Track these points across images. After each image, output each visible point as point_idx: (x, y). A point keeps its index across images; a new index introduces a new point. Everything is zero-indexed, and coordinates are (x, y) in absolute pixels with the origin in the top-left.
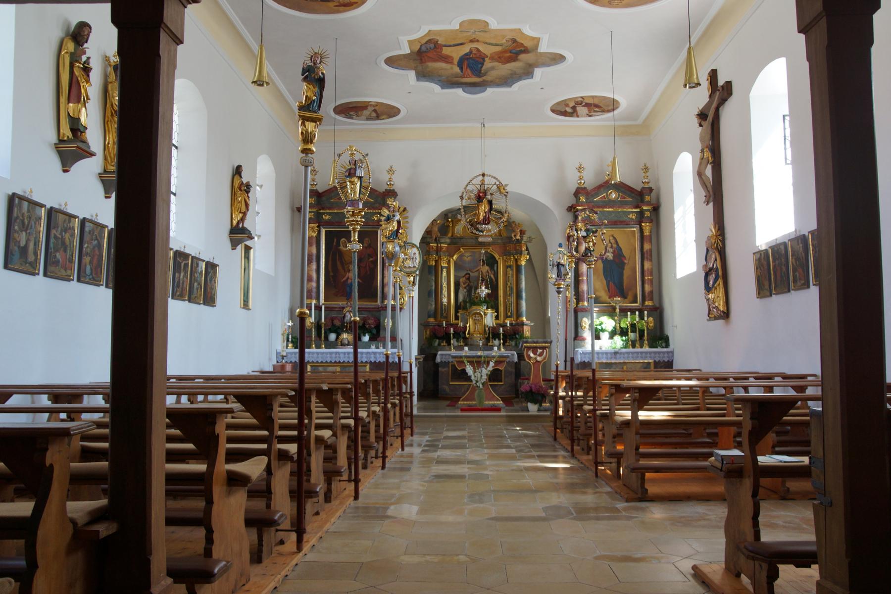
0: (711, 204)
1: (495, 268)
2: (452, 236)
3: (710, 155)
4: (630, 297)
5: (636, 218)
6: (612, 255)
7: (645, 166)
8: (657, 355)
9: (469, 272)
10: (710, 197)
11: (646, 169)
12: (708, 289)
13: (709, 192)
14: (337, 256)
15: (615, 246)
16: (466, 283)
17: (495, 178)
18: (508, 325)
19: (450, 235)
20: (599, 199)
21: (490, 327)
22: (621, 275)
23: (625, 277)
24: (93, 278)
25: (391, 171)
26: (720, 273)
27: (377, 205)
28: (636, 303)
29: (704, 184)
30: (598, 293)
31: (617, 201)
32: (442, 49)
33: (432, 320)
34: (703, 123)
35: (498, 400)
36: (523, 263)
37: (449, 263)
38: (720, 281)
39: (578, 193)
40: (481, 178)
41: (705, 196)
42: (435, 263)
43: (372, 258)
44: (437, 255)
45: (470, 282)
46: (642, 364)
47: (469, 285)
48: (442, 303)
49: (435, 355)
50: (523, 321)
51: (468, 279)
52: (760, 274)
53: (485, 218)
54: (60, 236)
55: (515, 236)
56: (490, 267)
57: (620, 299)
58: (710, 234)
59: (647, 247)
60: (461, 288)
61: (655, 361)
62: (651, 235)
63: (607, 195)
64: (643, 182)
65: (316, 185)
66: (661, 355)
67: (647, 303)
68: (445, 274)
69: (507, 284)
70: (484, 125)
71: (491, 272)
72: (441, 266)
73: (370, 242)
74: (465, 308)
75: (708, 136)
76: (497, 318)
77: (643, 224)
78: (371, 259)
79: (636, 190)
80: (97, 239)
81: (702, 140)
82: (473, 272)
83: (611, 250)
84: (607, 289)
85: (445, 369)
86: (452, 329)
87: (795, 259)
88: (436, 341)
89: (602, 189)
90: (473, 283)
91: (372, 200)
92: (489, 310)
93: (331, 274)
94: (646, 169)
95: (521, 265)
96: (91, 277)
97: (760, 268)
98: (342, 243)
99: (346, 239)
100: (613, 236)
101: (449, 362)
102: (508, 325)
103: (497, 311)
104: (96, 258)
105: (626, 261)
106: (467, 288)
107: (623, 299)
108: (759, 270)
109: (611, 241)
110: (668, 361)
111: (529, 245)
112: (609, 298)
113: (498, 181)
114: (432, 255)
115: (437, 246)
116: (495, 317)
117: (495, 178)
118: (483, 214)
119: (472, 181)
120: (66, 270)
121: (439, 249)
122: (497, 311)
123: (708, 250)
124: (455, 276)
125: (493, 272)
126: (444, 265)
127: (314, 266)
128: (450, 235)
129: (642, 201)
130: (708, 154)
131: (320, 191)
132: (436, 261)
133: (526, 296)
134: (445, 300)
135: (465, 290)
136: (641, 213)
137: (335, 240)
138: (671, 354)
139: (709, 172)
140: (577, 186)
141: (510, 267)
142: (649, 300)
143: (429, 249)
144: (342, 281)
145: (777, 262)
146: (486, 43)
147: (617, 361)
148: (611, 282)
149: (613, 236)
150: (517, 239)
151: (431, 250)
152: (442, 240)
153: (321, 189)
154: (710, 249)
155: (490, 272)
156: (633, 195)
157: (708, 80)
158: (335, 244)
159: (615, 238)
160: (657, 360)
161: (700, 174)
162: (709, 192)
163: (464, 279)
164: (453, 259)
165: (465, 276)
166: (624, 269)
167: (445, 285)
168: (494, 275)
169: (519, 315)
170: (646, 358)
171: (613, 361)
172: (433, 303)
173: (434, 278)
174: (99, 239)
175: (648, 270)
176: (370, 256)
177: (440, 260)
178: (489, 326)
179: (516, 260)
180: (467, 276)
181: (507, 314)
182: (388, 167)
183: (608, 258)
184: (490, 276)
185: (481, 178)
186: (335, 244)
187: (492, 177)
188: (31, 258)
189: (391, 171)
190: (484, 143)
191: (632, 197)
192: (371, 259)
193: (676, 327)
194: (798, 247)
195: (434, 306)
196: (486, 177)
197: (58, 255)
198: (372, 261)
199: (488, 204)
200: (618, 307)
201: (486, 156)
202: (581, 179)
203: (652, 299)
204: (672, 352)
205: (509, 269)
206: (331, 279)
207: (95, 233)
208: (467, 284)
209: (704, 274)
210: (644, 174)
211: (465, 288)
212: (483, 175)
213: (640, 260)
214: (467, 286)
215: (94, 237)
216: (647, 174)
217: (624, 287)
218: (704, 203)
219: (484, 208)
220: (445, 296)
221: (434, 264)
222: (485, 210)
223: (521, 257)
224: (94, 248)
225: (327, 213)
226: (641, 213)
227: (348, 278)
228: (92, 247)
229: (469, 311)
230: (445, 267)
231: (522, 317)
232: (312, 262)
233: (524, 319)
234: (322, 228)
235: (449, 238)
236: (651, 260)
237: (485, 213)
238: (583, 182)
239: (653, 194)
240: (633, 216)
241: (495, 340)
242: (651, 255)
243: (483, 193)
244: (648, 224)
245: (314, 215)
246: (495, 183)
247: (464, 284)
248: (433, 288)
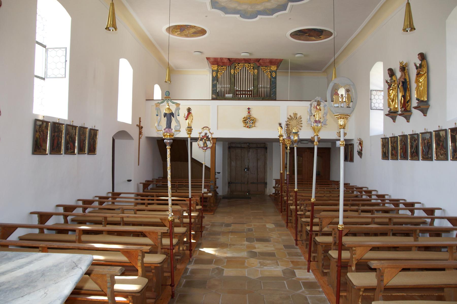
24: (404, 157)
52: (38, 137)
54: (393, 145)
80: (404, 142)
87: (69, 137)
96: (403, 157)
97: (39, 132)
104: (404, 149)
108: (38, 133)
120: (396, 157)
145: (56, 134)
174: (404, 141)
188: (387, 155)
194: (72, 131)
197: (393, 152)
207: (403, 140)
215: (403, 141)
224: (403, 145)
228: (402, 145)
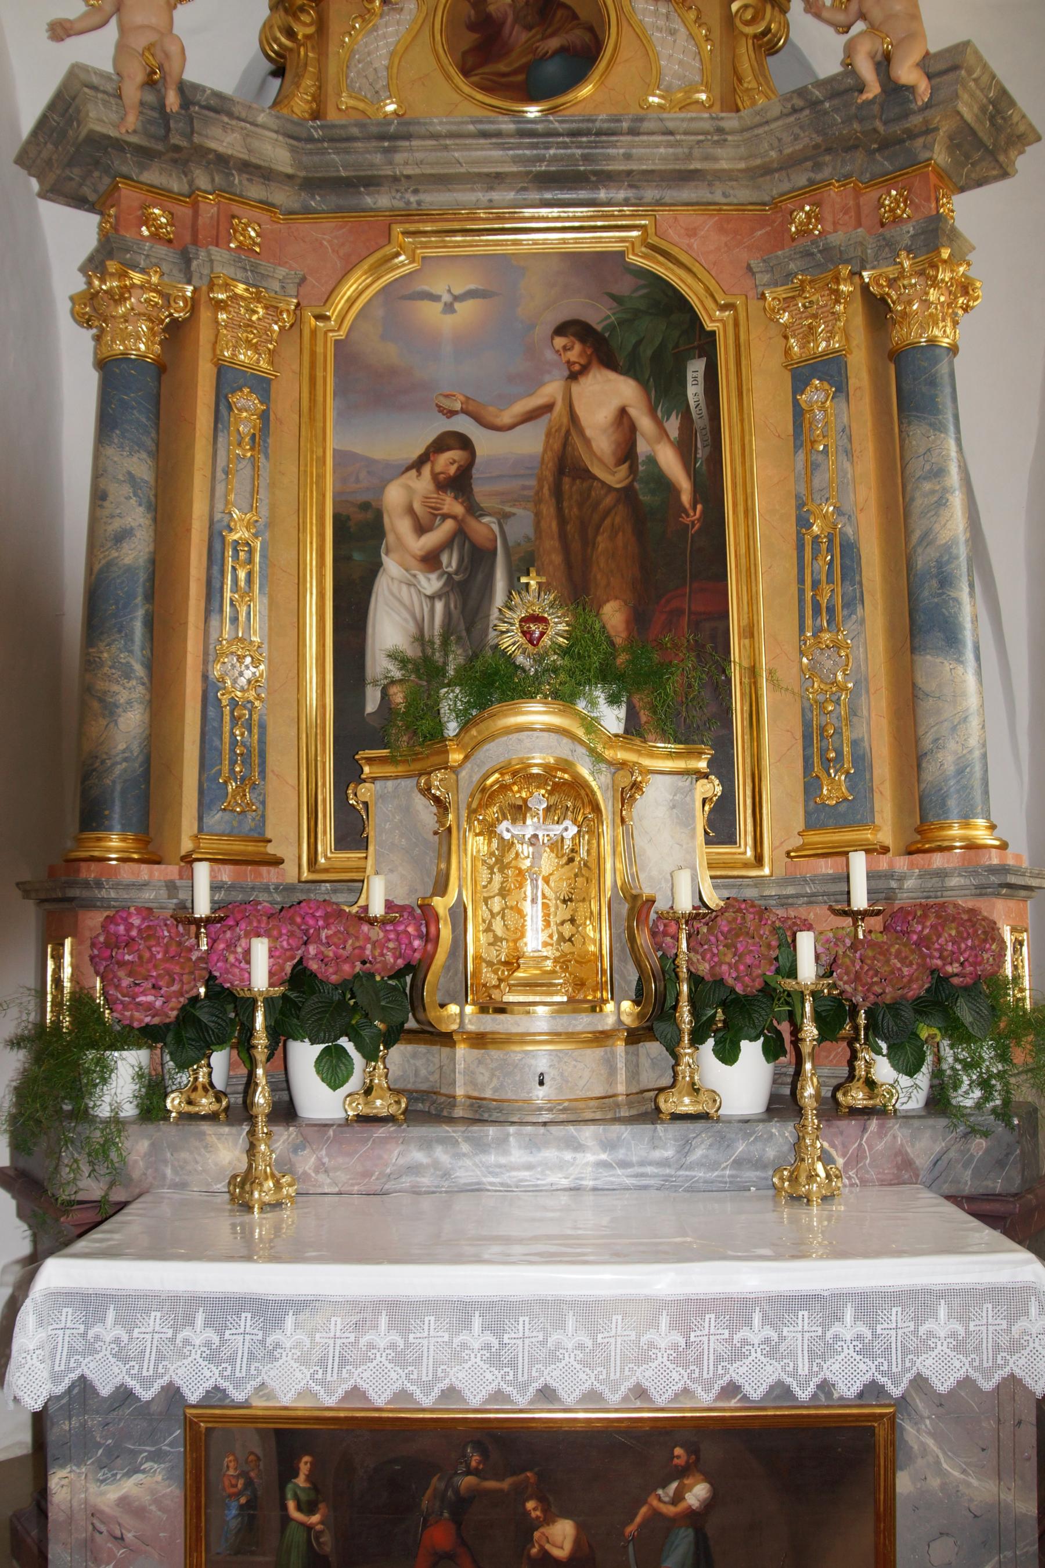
1: (694, 391)
9: (463, 425)
16: (437, 515)
18: (860, 901)
21: (672, 918)
45: (474, 509)
47: (460, 534)
48: (210, 689)
56: (643, 383)
60: (391, 566)
69: (803, 523)
71: (659, 424)
82: (511, 427)
85: (129, 1486)
86: (260, 949)
88: (105, 1071)
90: (503, 517)
102: (860, 901)
106: (450, 561)
116: (711, 822)
125: (673, 426)
126: (245, 356)
135: (431, 583)
155: (645, 423)
163: (422, 484)
165: (418, 464)
168: (685, 448)
177: (205, 314)
178: (661, 905)
180: (448, 461)
184: (652, 461)
205: (816, 394)
208: (449, 525)
211: (430, 560)
214: (447, 545)
230: (262, 386)
241: (728, 1054)
247: (421, 529)
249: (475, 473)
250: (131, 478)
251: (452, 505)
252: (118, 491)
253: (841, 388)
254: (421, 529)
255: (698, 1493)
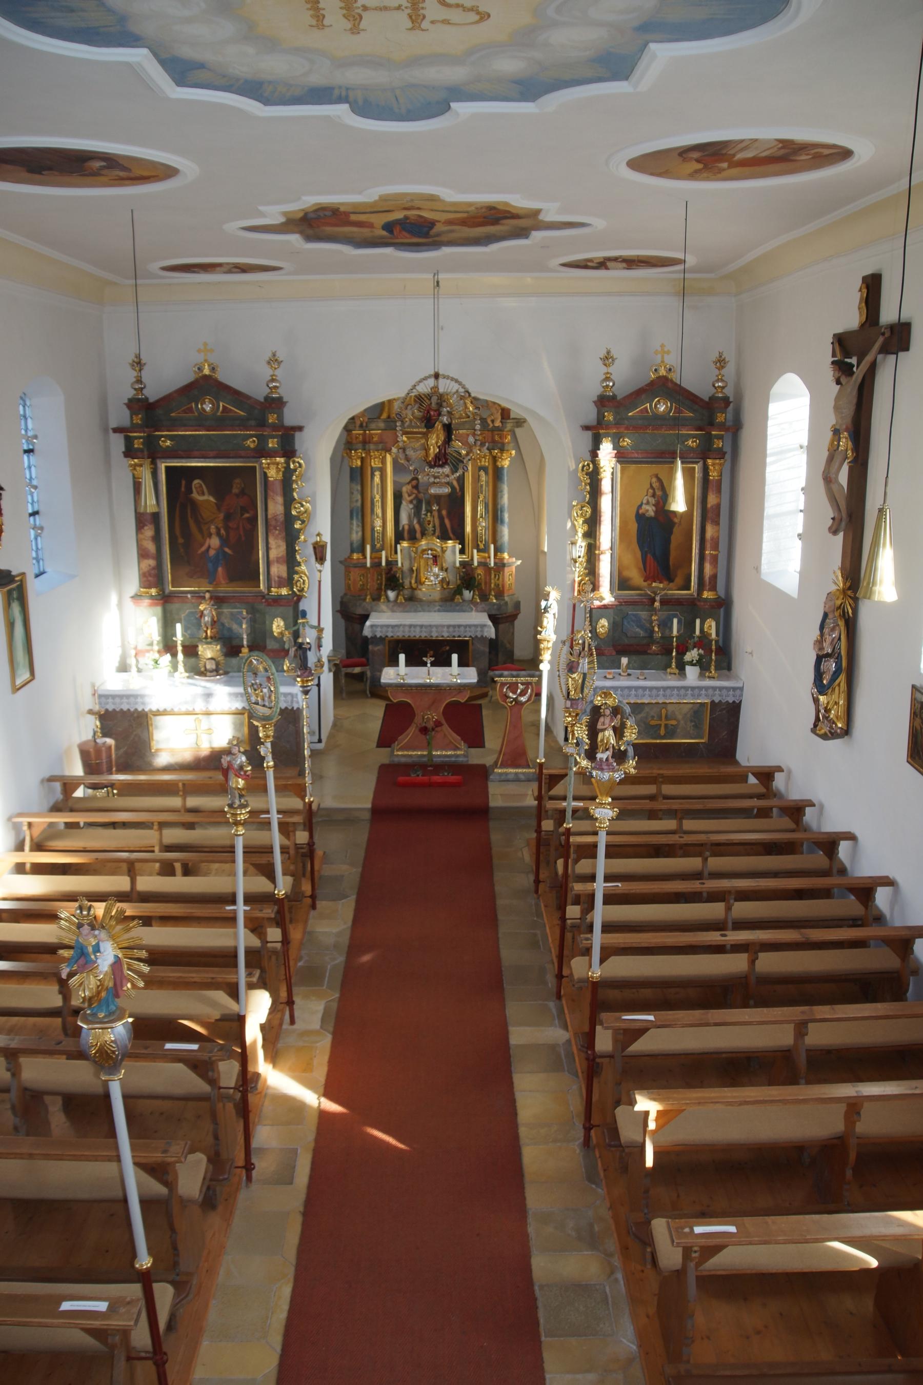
0: (841, 534)
2: (389, 417)
3: (850, 444)
4: (679, 580)
5: (698, 446)
6: (654, 508)
7: (721, 357)
8: (717, 692)
10: (841, 520)
11: (721, 362)
12: (820, 686)
13: (840, 510)
14: (189, 511)
15: (659, 493)
17: (457, 381)
19: (384, 416)
20: (638, 412)
22: (667, 542)
23: (673, 545)
25: (274, 361)
26: (844, 664)
27: (253, 423)
28: (689, 589)
29: (833, 499)
30: (626, 573)
31: (668, 417)
32: (349, 216)
33: (355, 556)
34: (843, 380)
35: (456, 748)
36: (506, 463)
37: (383, 461)
38: (842, 678)
39: (603, 401)
40: (431, 382)
41: (833, 519)
42: (362, 462)
43: (248, 513)
44: (364, 449)
45: (419, 492)
46: (691, 705)
47: (416, 498)
48: (373, 529)
49: (366, 617)
50: (504, 558)
51: (416, 487)
52: (919, 728)
53: (437, 457)
55: (493, 421)
57: (661, 586)
58: (834, 588)
59: (712, 500)
60: (404, 503)
61: (713, 702)
62: (721, 480)
63: (651, 406)
64: (714, 386)
65: (145, 387)
66: (724, 692)
67: (706, 595)
68: (377, 479)
70: (438, 282)
72: (372, 468)
73: (243, 486)
74: (413, 538)
75: (849, 411)
76: (462, 552)
77: (710, 461)
78: (247, 515)
79: (702, 400)
81: (836, 408)
83: (652, 500)
84: (642, 566)
89: (643, 396)
90: (424, 494)
91: (242, 413)
92: (450, 542)
93: (181, 541)
94: (721, 362)
95: (502, 468)
98: (196, 488)
99: (203, 481)
100: (657, 476)
101: (387, 636)
103: (462, 543)
105: (676, 520)
106: (415, 502)
107: (666, 583)
109: (654, 485)
110: (734, 702)
111: (518, 431)
112: (645, 581)
113: (463, 387)
114: (355, 450)
115: (364, 435)
117: (457, 381)
118: (434, 450)
119: (417, 388)
121: (367, 440)
122: (462, 543)
123: (826, 615)
124: (395, 483)
127: (149, 532)
128: (384, 416)
129: (711, 423)
130: (845, 443)
131: (151, 400)
132: (362, 459)
133: (509, 517)
134: (378, 523)
135: (411, 506)
136: (707, 440)
137: (183, 482)
138: (738, 692)
139: (843, 477)
140: (598, 390)
141: (485, 469)
142: (710, 590)
143: (351, 438)
144: (200, 552)
146: (432, 210)
147: (654, 701)
148: (649, 555)
149: (657, 476)
150: (494, 426)
151: (354, 441)
152: (373, 426)
153: (153, 393)
154: (830, 616)
156: (696, 407)
157: (860, 290)
158: (183, 489)
159: (659, 480)
160: (717, 701)
161: (829, 479)
162: (840, 510)
163: (409, 487)
164: (390, 454)
165: (408, 483)
166: (671, 533)
167: (378, 497)
169: (498, 550)
170: (699, 696)
171: (646, 701)
172: (360, 529)
173: (359, 488)
175: (712, 539)
176: (244, 510)
179: (495, 459)
180: (414, 482)
181: (478, 545)
182: (269, 355)
183: (647, 515)
185: (431, 382)
186: (183, 489)
187: (452, 379)
189: (274, 361)
190: (438, 305)
191: (693, 411)
192: (247, 515)
193: (751, 653)
195: (360, 534)
196: (441, 380)
198: (248, 519)
199: (444, 430)
200: (658, 598)
201: (442, 329)
202: (607, 379)
203: (713, 588)
204: (741, 689)
205: (482, 473)
206: (182, 550)
208: (414, 495)
209: (813, 658)
210: (717, 372)
211: (411, 502)
212: (437, 376)
213: (699, 519)
214: (414, 499)
216: (723, 372)
217: (671, 563)
218: (830, 528)
219: (435, 440)
220: (378, 517)
221: (359, 463)
222: (437, 443)
223: (502, 453)
225: (166, 436)
226: (707, 440)
227: (209, 547)
229: (416, 546)
231: (504, 552)
232: (145, 525)
233: (506, 555)
234: (158, 461)
235: (385, 421)
236: (717, 523)
237: (439, 447)
238: (611, 384)
239: (731, 408)
240: (692, 442)
242: (718, 515)
243: (435, 411)
244: (717, 461)
245: (143, 444)
246: (457, 391)
247: (409, 496)
248: (359, 504)
249: (420, 485)
250: (357, 490)
251: (415, 491)
252: (355, 493)
253: (487, 473)
254: (409, 496)
255: (448, 648)
